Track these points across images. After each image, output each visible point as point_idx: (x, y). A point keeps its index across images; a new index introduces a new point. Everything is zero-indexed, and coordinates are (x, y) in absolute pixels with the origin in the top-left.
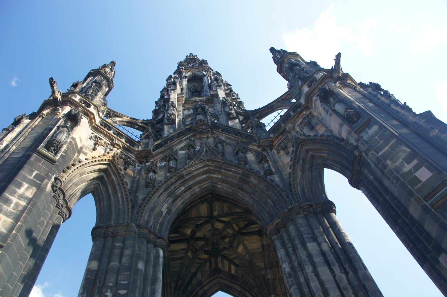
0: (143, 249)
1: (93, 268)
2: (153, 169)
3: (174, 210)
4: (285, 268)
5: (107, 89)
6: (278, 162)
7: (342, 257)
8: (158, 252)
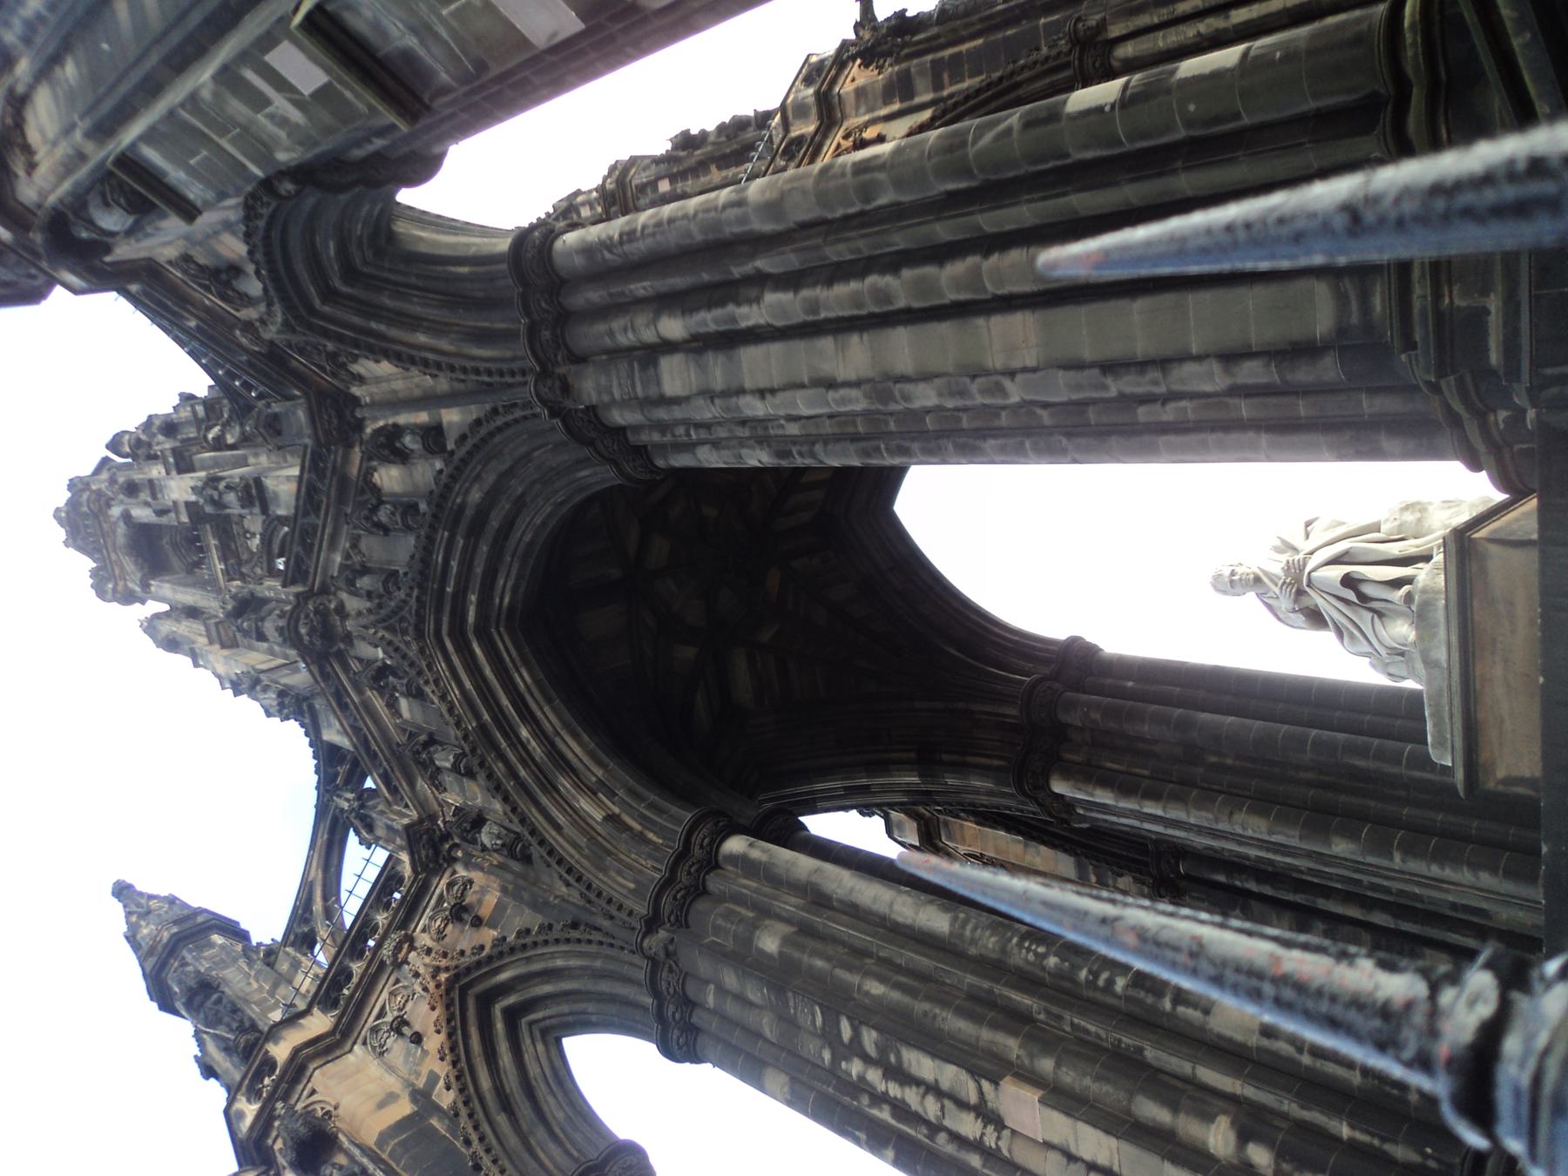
0: (720, 922)
1: (786, 1089)
2: (467, 825)
3: (600, 773)
5: (218, 939)
6: (395, 392)
7: (706, 277)
8: (735, 859)
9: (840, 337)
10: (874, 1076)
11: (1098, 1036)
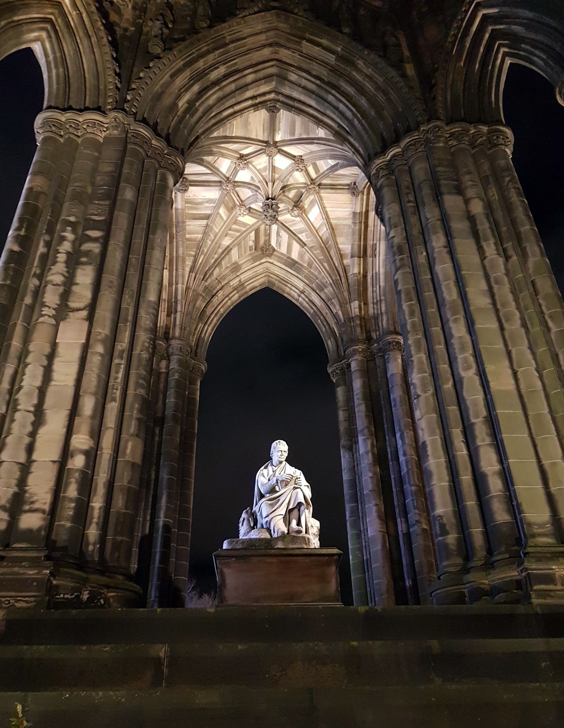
4: (394, 237)
7: (504, 229)
9: (488, 293)
10: (66, 246)
11: (116, 378)
